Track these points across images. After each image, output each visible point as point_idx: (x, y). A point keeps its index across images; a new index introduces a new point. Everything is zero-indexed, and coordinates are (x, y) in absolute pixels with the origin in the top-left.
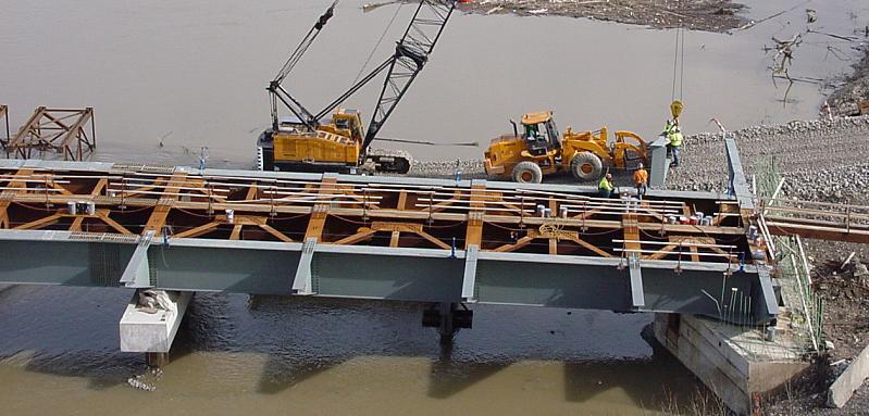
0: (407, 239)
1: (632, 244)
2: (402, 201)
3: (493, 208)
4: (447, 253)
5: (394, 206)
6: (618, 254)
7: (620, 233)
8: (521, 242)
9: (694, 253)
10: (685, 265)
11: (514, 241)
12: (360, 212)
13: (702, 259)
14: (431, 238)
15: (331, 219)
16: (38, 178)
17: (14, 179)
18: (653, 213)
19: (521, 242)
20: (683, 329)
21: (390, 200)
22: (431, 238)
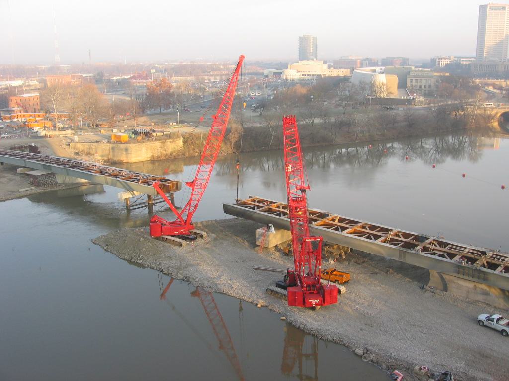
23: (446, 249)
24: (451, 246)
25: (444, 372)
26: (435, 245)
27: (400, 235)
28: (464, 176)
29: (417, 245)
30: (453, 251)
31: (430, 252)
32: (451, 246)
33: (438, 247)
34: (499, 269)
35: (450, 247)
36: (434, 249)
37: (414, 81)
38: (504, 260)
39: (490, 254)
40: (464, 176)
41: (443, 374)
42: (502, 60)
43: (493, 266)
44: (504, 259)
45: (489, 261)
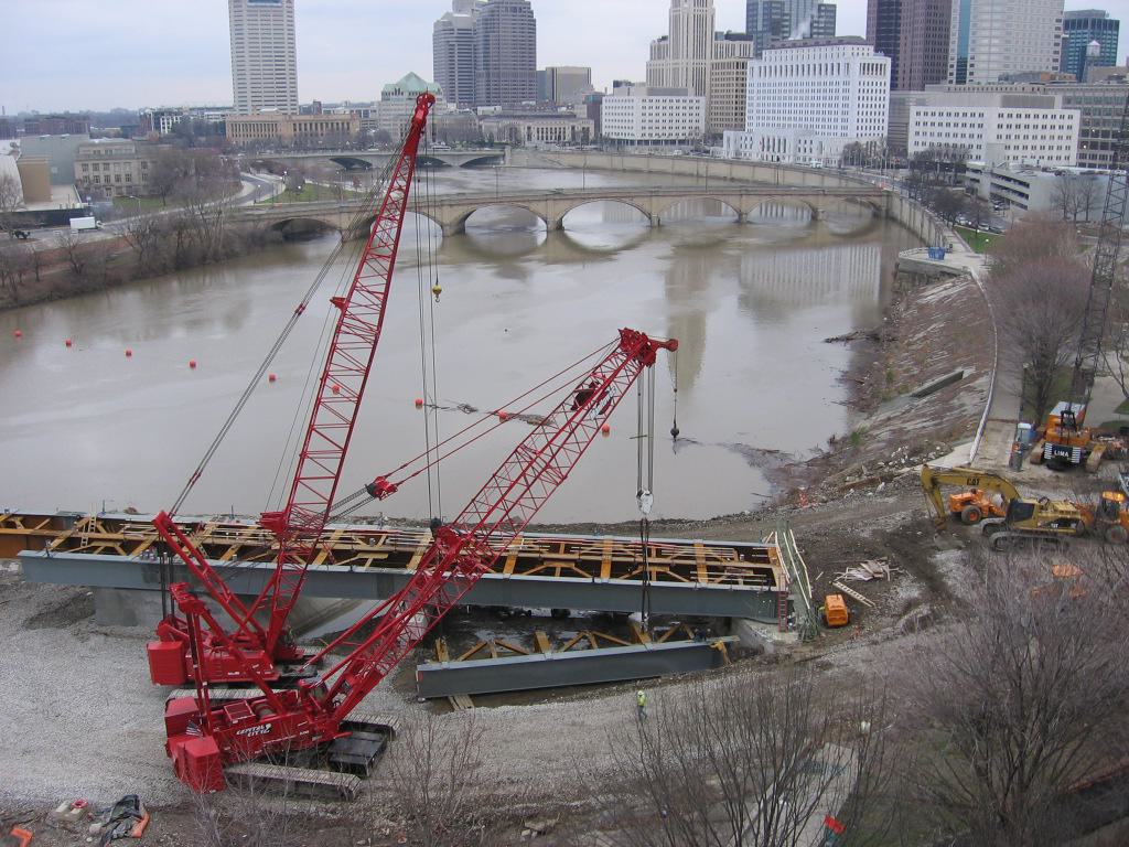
0: (565, 572)
1: (702, 572)
2: (562, 548)
3: (615, 553)
4: (589, 580)
5: (557, 551)
6: (692, 580)
7: (694, 568)
8: (634, 573)
9: (741, 580)
10: (735, 587)
11: (630, 573)
12: (537, 555)
13: (745, 583)
14: (581, 572)
15: (519, 560)
16: (347, 535)
17: (333, 535)
18: (715, 555)
19: (634, 573)
20: (733, 626)
21: (554, 547)
22: (581, 572)
23: (118, 536)
24: (128, 526)
25: (120, 799)
26: (98, 531)
27: (18, 523)
28: (193, 365)
29: (52, 538)
30: (132, 536)
31: (82, 547)
32: (128, 526)
33: (104, 534)
34: (231, 553)
35: (128, 529)
36: (91, 540)
37: (101, 167)
38: (241, 534)
39: (211, 526)
40: (193, 365)
41: (120, 804)
42: (289, 112)
43: (216, 551)
44: (242, 531)
45: (209, 541)
